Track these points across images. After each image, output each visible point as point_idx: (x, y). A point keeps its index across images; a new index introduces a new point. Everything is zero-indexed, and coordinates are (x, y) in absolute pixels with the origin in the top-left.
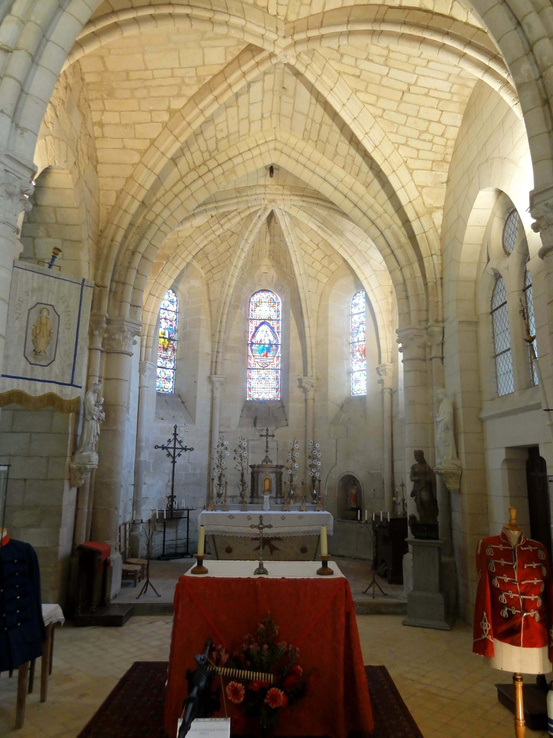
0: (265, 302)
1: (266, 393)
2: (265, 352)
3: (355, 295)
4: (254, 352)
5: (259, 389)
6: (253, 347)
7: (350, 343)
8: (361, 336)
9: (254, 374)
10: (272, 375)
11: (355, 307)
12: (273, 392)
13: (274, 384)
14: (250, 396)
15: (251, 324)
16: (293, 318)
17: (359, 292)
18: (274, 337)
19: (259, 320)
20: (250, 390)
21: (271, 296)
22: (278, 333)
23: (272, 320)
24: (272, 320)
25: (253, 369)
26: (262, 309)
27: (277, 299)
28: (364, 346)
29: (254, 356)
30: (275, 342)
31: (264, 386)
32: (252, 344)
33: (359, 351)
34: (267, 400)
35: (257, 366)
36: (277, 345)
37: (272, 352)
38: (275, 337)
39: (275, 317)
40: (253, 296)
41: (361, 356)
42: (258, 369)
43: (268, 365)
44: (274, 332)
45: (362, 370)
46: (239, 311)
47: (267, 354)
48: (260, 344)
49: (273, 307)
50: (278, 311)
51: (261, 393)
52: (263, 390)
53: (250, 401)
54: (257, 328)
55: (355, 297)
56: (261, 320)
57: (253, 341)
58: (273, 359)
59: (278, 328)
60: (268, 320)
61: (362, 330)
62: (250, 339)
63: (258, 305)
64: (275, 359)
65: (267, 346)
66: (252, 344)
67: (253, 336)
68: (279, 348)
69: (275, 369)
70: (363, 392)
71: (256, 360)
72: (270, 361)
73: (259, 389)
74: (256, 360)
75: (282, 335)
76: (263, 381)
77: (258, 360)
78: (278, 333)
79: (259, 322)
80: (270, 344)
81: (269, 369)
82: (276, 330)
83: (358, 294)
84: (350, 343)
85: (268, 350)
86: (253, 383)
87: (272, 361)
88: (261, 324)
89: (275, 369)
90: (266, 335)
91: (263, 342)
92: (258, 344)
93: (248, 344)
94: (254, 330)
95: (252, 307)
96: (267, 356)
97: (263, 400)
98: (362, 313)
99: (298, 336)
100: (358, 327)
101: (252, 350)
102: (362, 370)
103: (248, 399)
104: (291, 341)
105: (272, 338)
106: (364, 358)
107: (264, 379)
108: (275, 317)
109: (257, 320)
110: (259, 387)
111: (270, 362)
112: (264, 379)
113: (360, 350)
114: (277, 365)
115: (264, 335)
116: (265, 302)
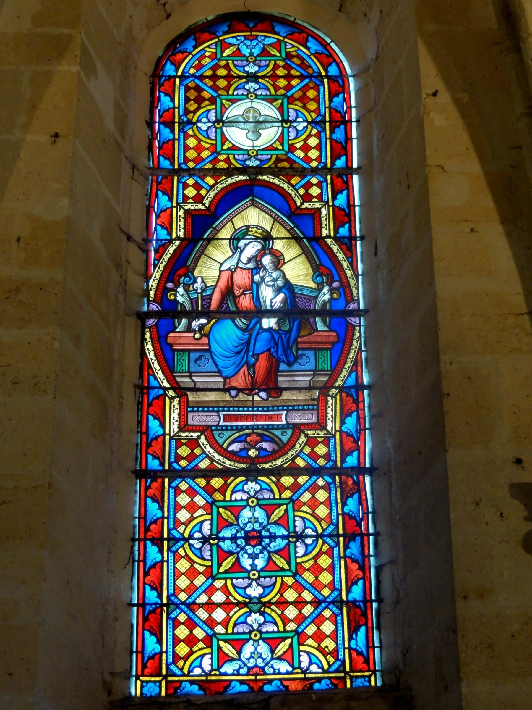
0: (253, 77)
1: (273, 643)
2: (262, 365)
4: (181, 364)
5: (219, 615)
6: (181, 334)
9: (186, 511)
10: (320, 507)
12: (328, 628)
13: (330, 574)
14: (152, 665)
15: (163, 200)
16: (444, 97)
18: (318, 270)
19: (216, 173)
20: (152, 619)
21: (291, 46)
22: (347, 244)
23: (302, 173)
24: (302, 173)
25: (174, 474)
26: (235, 111)
27: (327, 57)
29: (181, 392)
30: (325, 295)
31: (255, 591)
32: (171, 312)
34: (285, 693)
35: (208, 456)
36: (339, 316)
37: (309, 361)
38: (325, 268)
39: (314, 150)
40: (174, 49)
42: (209, 474)
43: (282, 449)
44: (317, 239)
46: (68, 68)
47: (273, 372)
48: (223, 313)
49: (304, 100)
50: (339, 120)
51: (238, 645)
52: (255, 619)
53: (148, 701)
54: (201, 227)
56: (230, 172)
57: (181, 296)
58: (320, 408)
59: (343, 216)
60: (276, 172)
62: (153, 283)
63: (206, 95)
64: (333, 407)
65: (269, 323)
66: (171, 312)
67: (181, 267)
68: (359, 335)
69: (332, 471)
71: (195, 419)
72: (297, 419)
73: (219, 615)
74: (195, 419)
75: (373, 252)
76: (252, 560)
77: (210, 419)
78: (347, 244)
79: (212, 188)
80: (296, 308)
81: (294, 471)
82: (326, 229)
85: (284, 350)
86: (181, 575)
87: (311, 418)
88: (230, 199)
89: (332, 471)
90: (267, 260)
91: (246, 302)
92: (206, 313)
93: (142, 317)
94: (180, 229)
95: (172, 102)
96: (275, 390)
97: (256, 688)
99: (487, 201)
101: (167, 356)
103: (135, 689)
104: (445, 237)
105: (298, 271)
107: (254, 538)
108: (314, 150)
109: (203, 173)
110: (219, 597)
111: (298, 429)
112: (254, 538)
114: (352, 442)
115: (253, 259)
116: (253, 77)
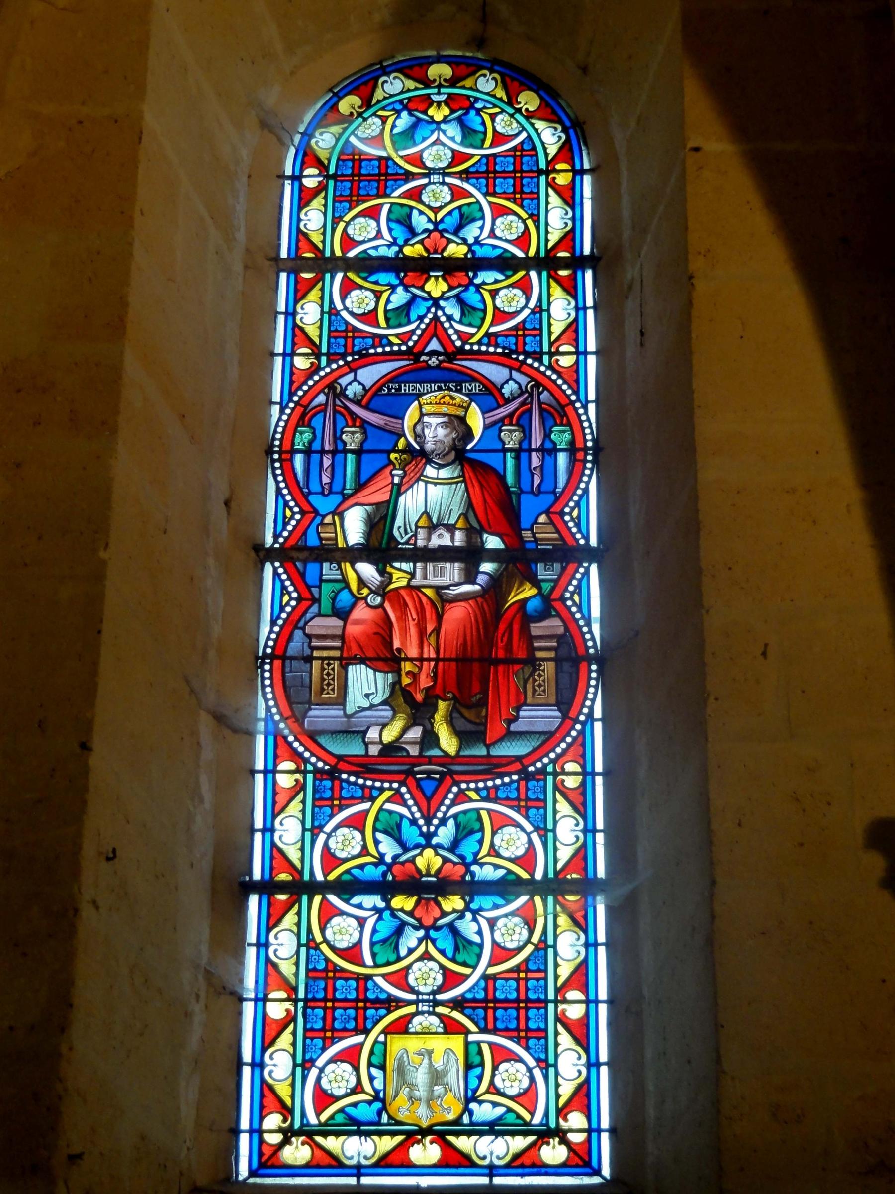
3: (364, 86)
7: (263, 555)
8: (431, 498)
11: (353, 198)
17: (415, 69)
28: (456, 614)
33: (386, 659)
41: (420, 712)
45: (413, 884)
55: (348, 104)
61: (436, 433)
70: (426, 1153)
83: (394, 85)
84: (263, 555)
98: (451, 268)
100: (388, 398)
102: (413, 884)
106: (448, 743)
113: (406, 641)
